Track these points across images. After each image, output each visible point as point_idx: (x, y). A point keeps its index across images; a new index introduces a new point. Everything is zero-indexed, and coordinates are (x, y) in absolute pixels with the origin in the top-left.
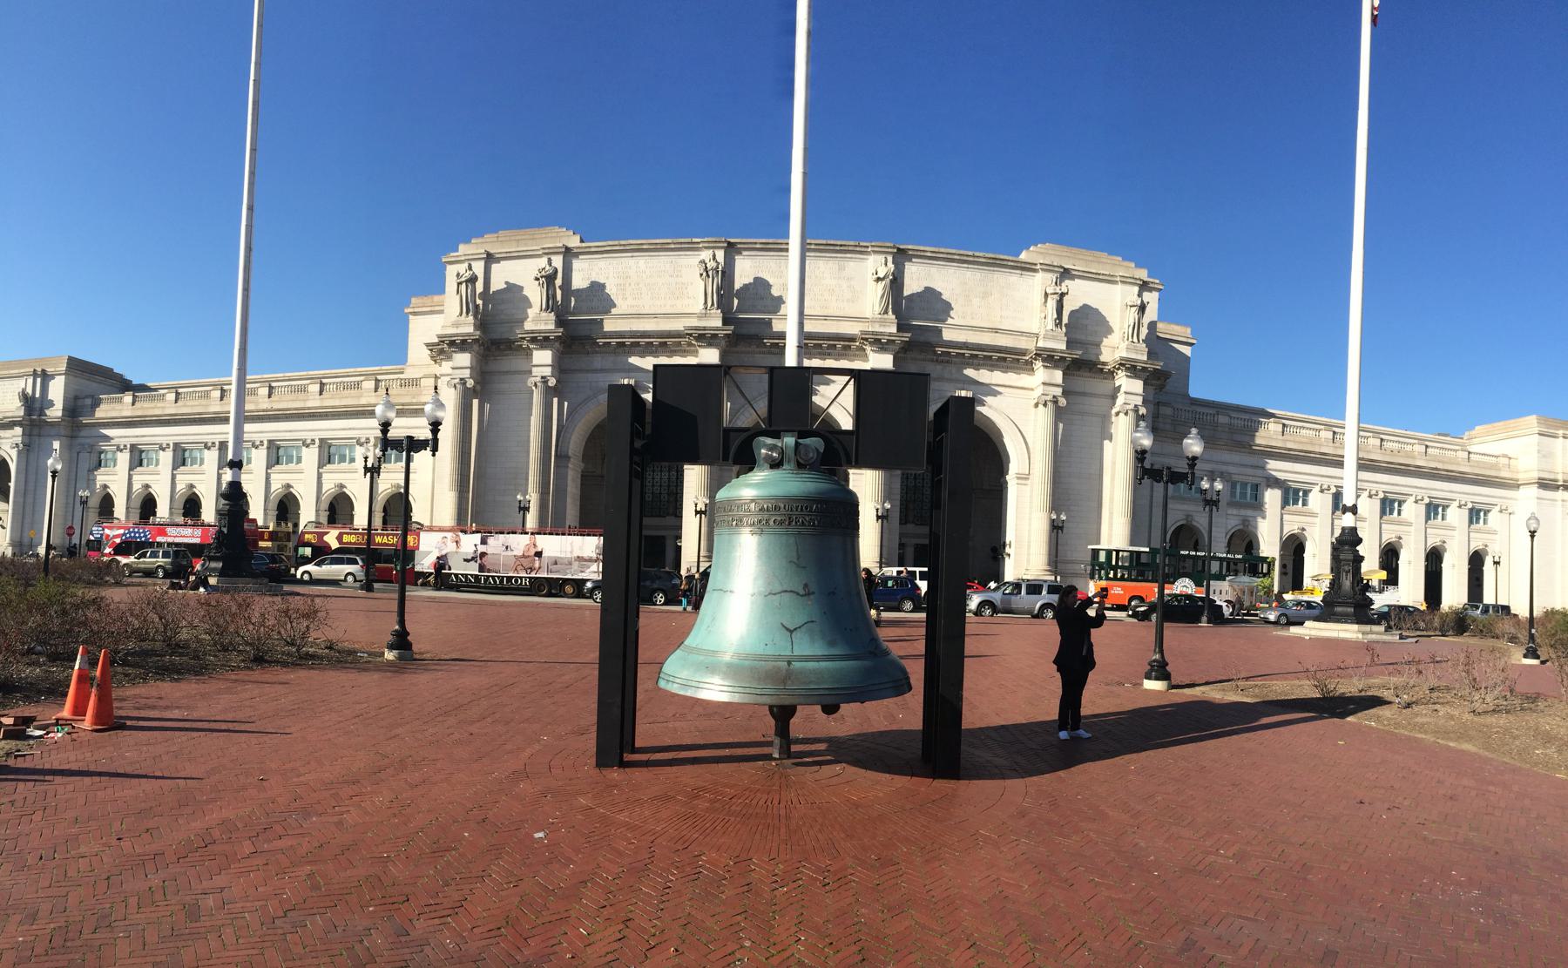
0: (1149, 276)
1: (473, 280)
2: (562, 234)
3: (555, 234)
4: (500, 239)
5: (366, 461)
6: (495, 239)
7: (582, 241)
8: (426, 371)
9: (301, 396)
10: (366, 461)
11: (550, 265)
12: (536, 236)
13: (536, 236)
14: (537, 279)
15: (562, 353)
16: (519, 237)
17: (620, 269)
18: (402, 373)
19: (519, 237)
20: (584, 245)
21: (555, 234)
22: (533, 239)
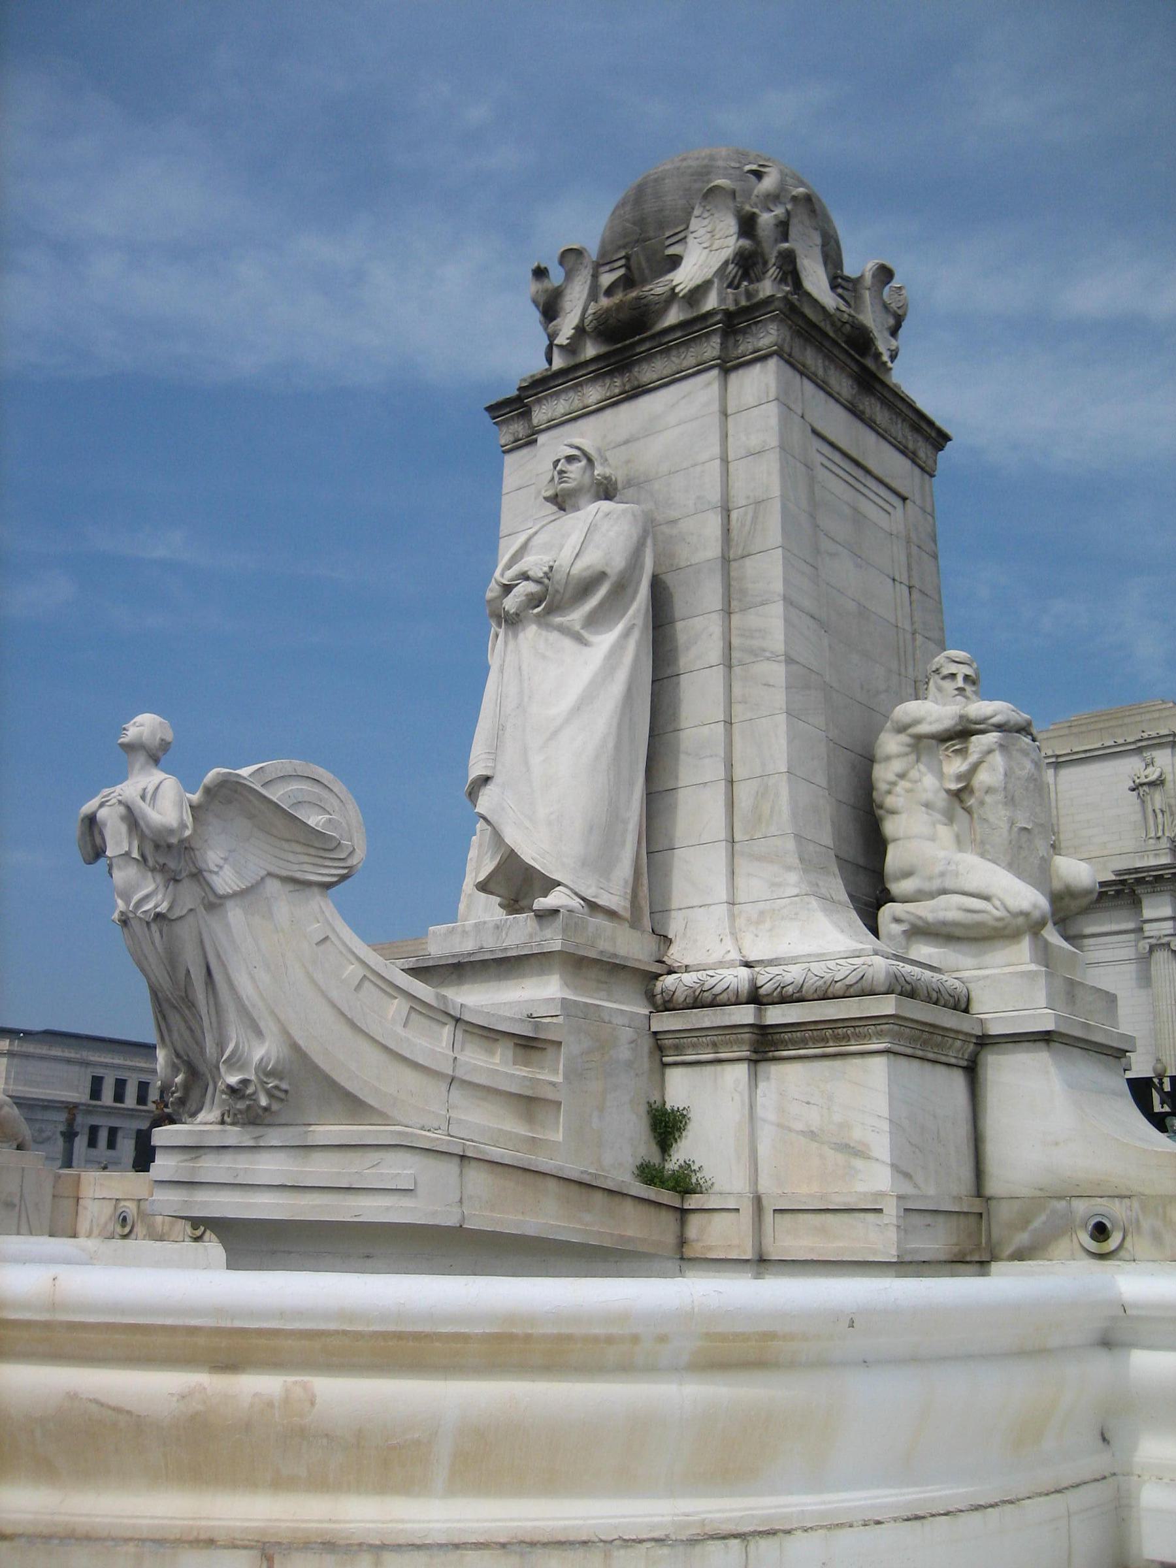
3: (1156, 715)
12: (1127, 720)
14: (1133, 790)
16: (1101, 725)
19: (1101, 725)
21: (1156, 715)
22: (1121, 726)
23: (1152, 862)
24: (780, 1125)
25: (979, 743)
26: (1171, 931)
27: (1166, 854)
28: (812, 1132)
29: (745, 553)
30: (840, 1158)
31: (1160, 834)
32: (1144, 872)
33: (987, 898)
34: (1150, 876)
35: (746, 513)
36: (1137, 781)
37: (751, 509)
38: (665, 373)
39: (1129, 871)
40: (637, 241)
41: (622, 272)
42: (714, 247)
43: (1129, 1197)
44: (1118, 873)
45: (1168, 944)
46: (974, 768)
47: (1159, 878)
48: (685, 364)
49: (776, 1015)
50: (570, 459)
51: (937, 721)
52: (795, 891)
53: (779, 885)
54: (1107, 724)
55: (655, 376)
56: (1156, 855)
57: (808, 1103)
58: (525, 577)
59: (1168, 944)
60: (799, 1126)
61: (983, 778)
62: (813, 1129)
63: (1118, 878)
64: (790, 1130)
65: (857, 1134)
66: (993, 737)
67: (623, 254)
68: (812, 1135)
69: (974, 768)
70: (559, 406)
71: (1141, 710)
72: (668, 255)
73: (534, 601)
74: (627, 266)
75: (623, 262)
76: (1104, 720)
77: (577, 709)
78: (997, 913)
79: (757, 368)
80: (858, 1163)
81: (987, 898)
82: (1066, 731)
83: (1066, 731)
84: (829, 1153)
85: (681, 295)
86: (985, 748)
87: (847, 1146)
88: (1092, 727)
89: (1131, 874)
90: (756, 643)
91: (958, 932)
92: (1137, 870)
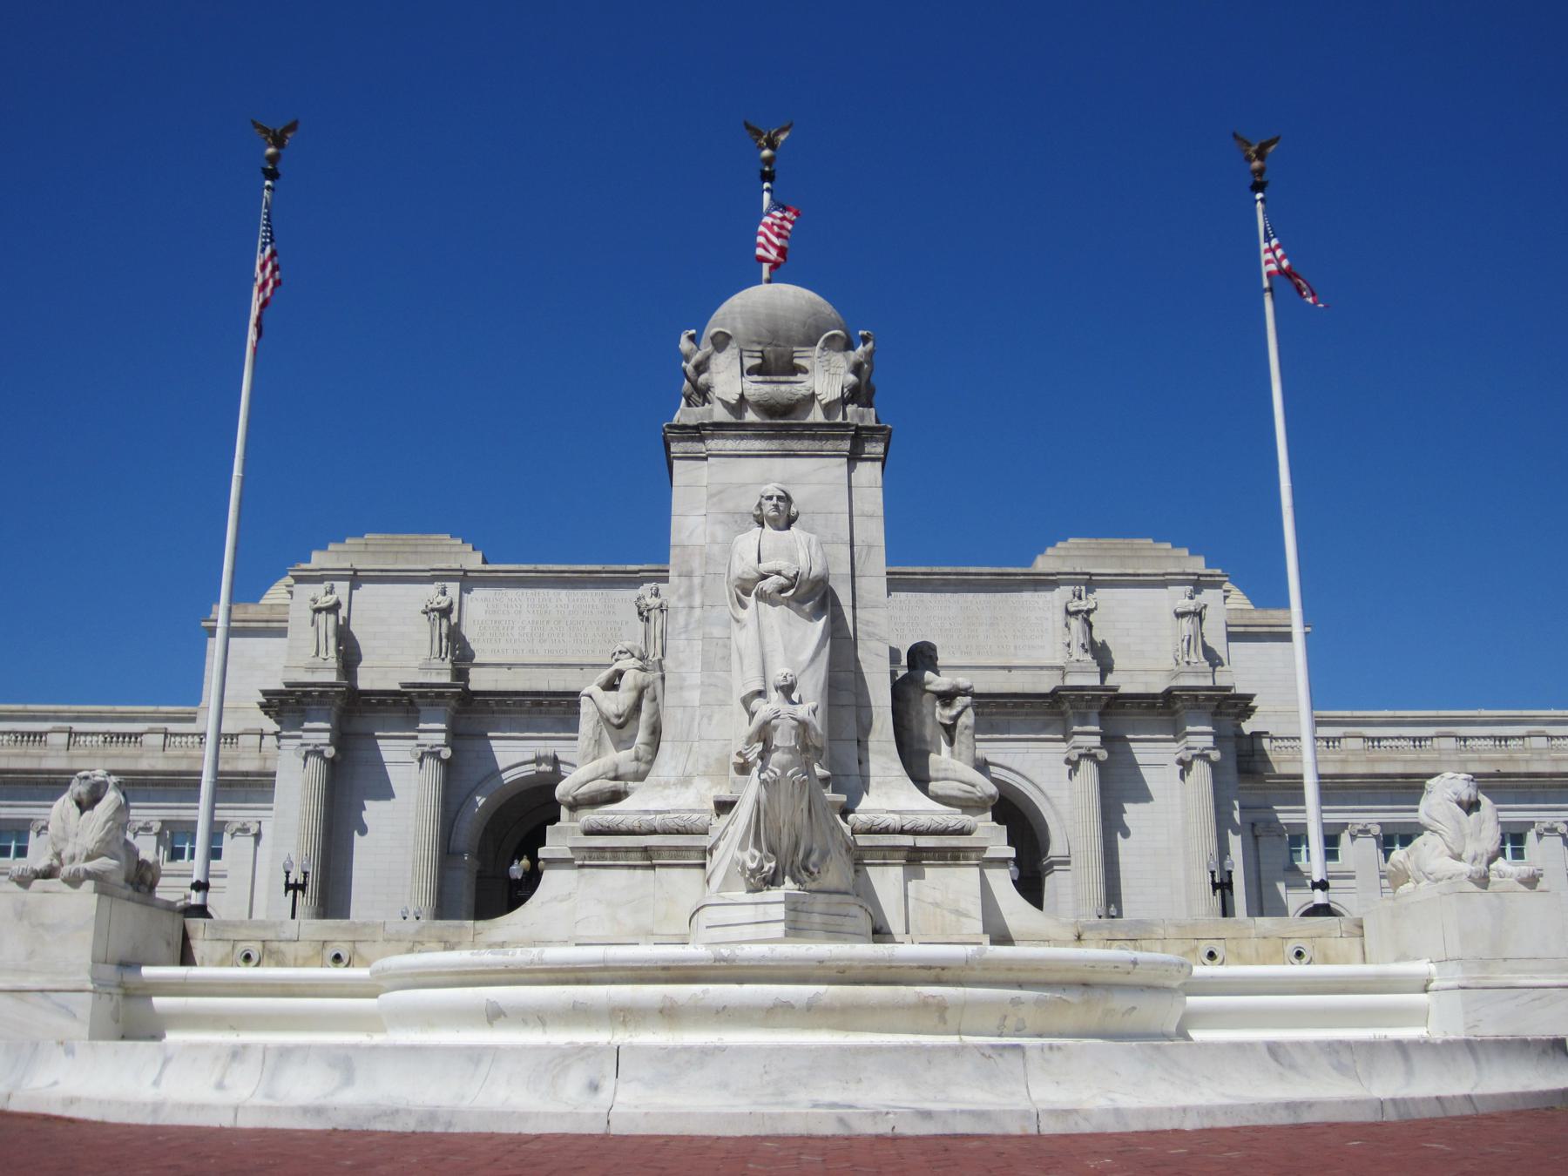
0: (1207, 567)
1: (337, 605)
2: (454, 549)
3: (446, 549)
4: (370, 548)
5: (287, 877)
6: (362, 548)
7: (485, 561)
8: (255, 725)
9: (34, 750)
10: (287, 877)
11: (444, 593)
12: (420, 549)
13: (420, 549)
14: (426, 613)
15: (457, 712)
17: (536, 602)
18: (193, 720)
20: (488, 567)
21: (446, 549)
22: (416, 552)
23: (434, 679)
24: (917, 899)
25: (961, 701)
26: (443, 742)
27: (447, 673)
28: (937, 903)
29: (862, 574)
30: (953, 917)
31: (443, 655)
32: (427, 687)
33: (973, 786)
34: (433, 692)
35: (862, 550)
36: (430, 606)
37: (866, 548)
38: (810, 448)
39: (414, 685)
40: (770, 344)
41: (758, 361)
42: (832, 372)
43: (1048, 941)
44: (404, 685)
45: (439, 752)
46: (960, 714)
47: (440, 695)
48: (825, 448)
49: (923, 842)
50: (779, 498)
51: (938, 685)
52: (899, 774)
53: (888, 769)
54: (402, 549)
55: (803, 448)
56: (438, 673)
57: (934, 888)
58: (779, 573)
59: (439, 752)
60: (930, 900)
61: (963, 720)
62: (938, 901)
63: (403, 690)
64: (923, 901)
65: (963, 905)
66: (968, 699)
67: (759, 348)
68: (936, 905)
69: (960, 714)
70: (729, 445)
71: (433, 542)
72: (796, 364)
73: (782, 590)
74: (763, 358)
75: (759, 354)
76: (399, 545)
77: (813, 660)
78: (979, 794)
79: (869, 464)
80: (963, 919)
81: (973, 786)
82: (362, 548)
83: (362, 548)
84: (945, 912)
85: (823, 402)
86: (965, 704)
87: (957, 911)
88: (388, 549)
89: (415, 687)
90: (870, 629)
91: (954, 802)
92: (421, 685)
